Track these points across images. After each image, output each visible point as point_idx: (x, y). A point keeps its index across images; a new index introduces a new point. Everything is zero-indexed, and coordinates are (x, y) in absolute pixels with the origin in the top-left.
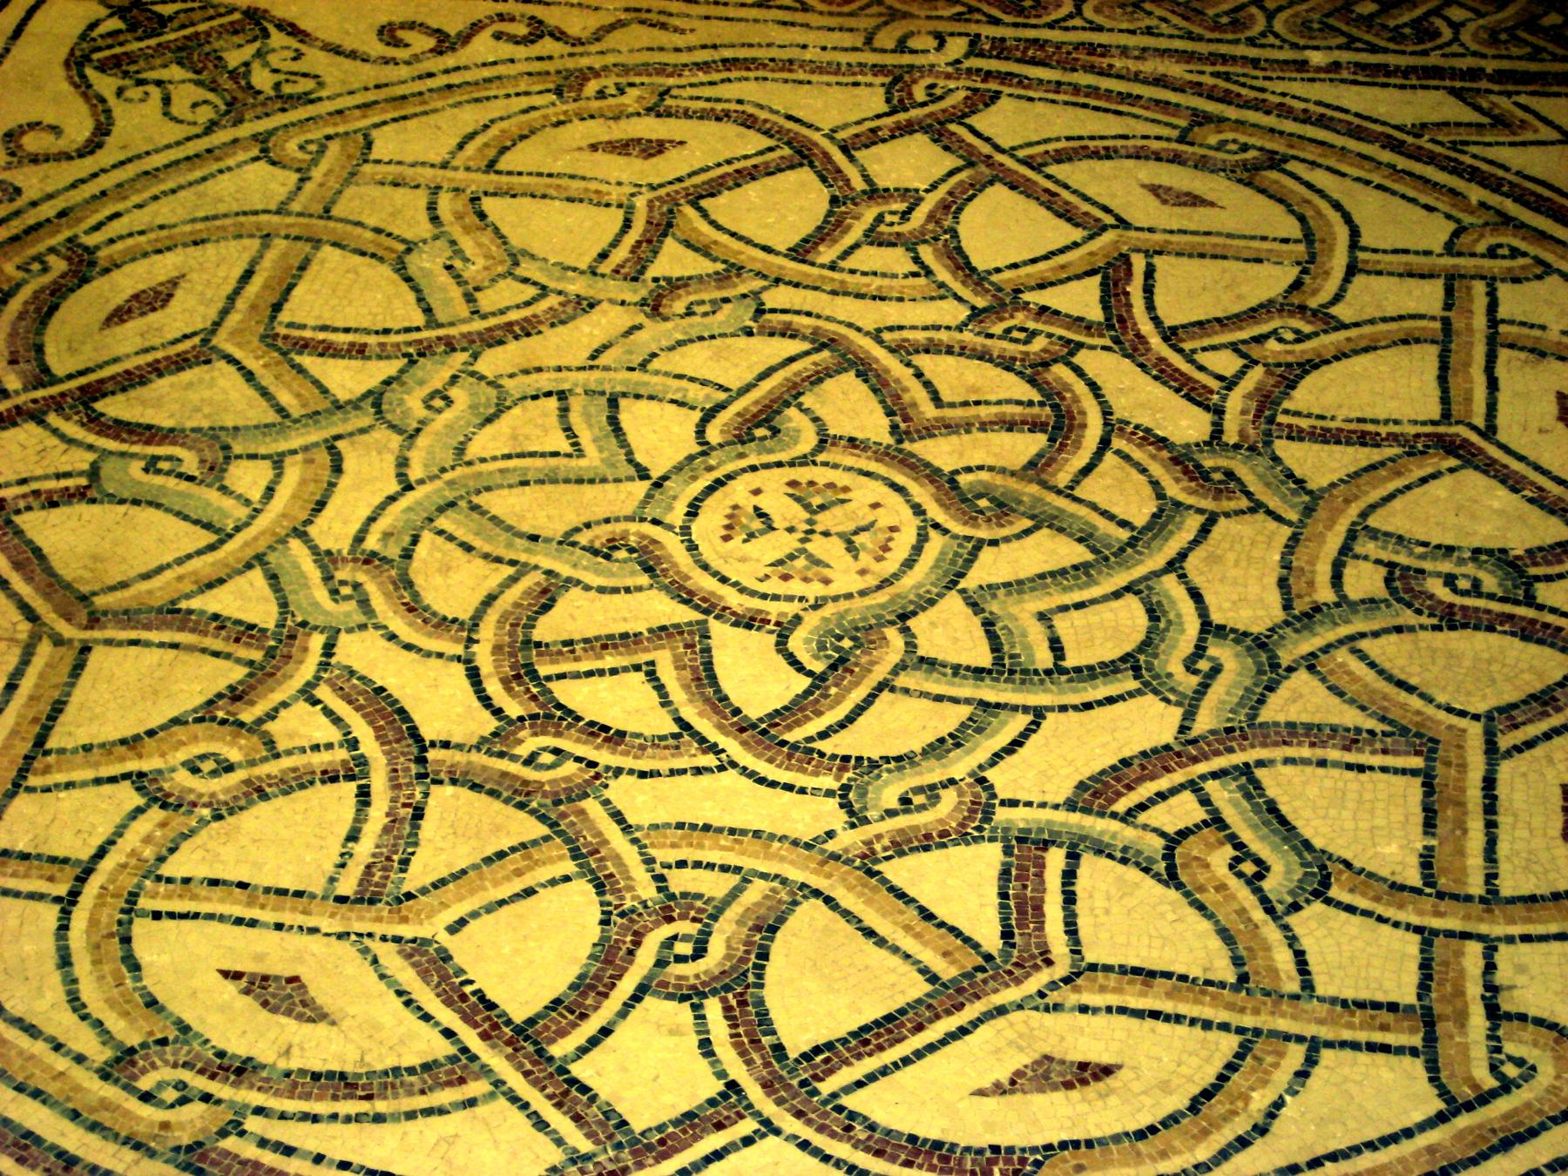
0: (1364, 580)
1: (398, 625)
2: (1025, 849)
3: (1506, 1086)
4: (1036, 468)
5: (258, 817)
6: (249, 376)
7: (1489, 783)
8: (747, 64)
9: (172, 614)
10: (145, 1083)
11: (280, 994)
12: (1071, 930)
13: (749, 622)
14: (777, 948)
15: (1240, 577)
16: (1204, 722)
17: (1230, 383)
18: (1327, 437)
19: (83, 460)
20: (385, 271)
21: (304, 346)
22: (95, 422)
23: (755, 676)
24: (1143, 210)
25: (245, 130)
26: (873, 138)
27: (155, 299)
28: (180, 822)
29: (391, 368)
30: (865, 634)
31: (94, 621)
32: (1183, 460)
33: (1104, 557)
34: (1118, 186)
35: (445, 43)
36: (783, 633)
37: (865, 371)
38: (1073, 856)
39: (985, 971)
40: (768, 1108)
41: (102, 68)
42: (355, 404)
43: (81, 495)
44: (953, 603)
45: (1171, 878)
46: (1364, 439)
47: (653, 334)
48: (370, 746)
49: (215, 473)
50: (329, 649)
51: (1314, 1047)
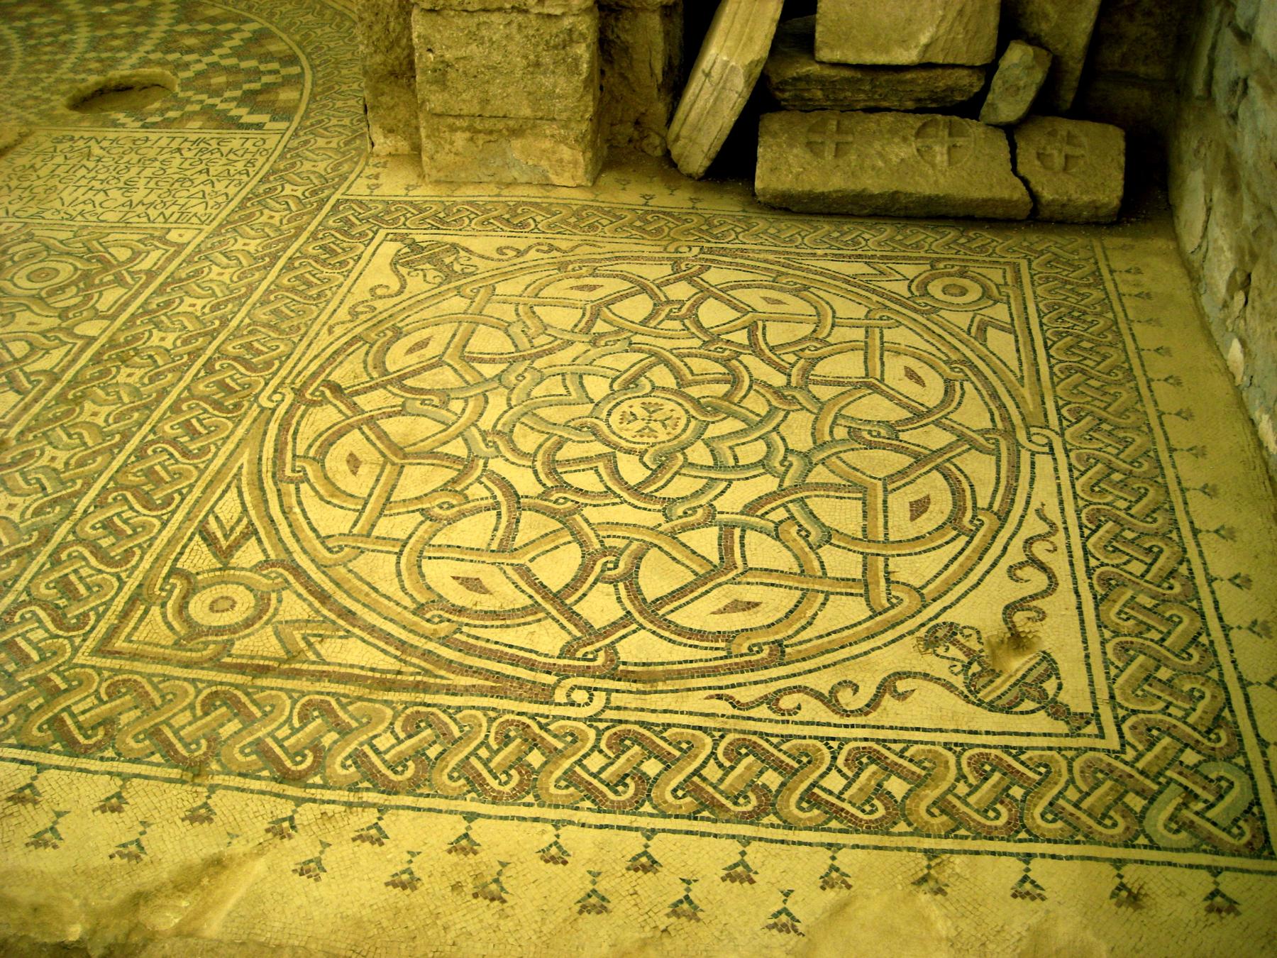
0: (841, 433)
1: (509, 455)
3: (893, 606)
4: (727, 396)
5: (463, 524)
7: (885, 502)
8: (624, 258)
9: (432, 454)
10: (428, 616)
11: (472, 584)
12: (744, 556)
15: (798, 432)
16: (787, 484)
17: (793, 365)
19: (399, 401)
20: (501, 333)
21: (474, 359)
22: (403, 387)
23: (633, 471)
24: (761, 306)
25: (452, 285)
26: (668, 283)
27: (423, 344)
28: (437, 525)
30: (670, 456)
31: (405, 456)
33: (752, 427)
34: (752, 297)
35: (520, 253)
36: (642, 455)
37: (667, 363)
38: (743, 531)
39: (714, 572)
40: (641, 620)
43: (399, 413)
44: (700, 443)
45: (777, 538)
46: (839, 384)
47: (594, 352)
48: (500, 498)
49: (445, 404)
50: (485, 465)
51: (827, 594)
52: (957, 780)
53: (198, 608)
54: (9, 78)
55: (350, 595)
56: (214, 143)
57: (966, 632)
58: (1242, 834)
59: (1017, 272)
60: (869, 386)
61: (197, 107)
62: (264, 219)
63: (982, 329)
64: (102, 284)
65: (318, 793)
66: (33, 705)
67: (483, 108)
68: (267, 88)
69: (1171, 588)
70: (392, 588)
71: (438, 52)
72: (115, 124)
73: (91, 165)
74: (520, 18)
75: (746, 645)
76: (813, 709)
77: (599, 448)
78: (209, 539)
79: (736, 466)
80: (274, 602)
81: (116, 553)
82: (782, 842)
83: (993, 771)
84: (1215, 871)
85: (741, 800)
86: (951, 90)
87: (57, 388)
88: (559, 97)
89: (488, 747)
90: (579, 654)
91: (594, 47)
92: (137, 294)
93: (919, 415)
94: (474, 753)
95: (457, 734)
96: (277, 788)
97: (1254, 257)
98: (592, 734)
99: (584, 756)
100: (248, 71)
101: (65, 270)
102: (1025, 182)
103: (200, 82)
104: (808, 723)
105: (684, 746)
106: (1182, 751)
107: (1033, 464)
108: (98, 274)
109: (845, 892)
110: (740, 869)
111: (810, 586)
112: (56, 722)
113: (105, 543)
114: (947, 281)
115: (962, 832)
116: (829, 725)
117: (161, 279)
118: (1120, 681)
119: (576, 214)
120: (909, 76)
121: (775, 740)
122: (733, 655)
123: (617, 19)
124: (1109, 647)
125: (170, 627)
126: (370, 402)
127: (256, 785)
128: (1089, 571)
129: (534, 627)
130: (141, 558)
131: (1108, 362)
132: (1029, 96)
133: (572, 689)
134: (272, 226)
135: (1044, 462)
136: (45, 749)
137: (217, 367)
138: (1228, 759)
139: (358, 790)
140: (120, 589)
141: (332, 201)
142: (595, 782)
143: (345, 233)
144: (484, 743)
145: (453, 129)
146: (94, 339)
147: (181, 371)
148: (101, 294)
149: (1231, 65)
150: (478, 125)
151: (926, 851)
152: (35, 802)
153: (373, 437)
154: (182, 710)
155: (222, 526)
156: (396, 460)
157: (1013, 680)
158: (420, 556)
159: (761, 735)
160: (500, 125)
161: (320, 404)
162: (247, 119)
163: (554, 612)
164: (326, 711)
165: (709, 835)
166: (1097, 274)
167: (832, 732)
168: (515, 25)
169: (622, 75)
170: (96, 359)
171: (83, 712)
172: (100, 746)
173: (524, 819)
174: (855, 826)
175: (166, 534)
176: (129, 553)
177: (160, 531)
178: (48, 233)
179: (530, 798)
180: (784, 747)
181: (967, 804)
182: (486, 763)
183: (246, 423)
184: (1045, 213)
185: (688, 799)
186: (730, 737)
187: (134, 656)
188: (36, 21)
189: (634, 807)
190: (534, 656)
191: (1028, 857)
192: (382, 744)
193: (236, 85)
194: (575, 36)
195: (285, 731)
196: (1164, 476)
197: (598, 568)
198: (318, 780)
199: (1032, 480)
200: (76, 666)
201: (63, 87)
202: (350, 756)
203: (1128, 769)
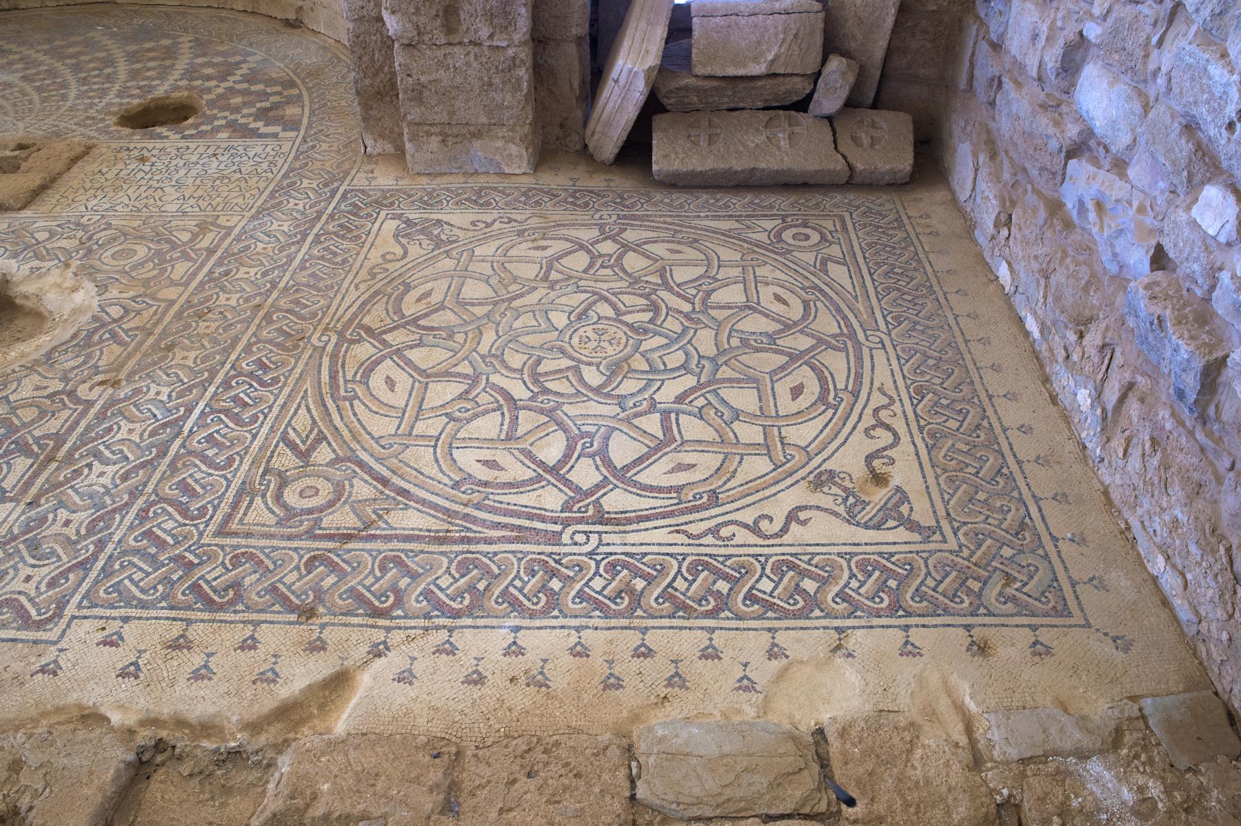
0: (735, 342)
1: (503, 371)
2: (666, 414)
3: (788, 461)
4: (652, 321)
7: (773, 389)
8: (564, 225)
9: (447, 374)
11: (491, 464)
12: (680, 432)
13: (589, 364)
14: (610, 443)
15: (705, 341)
16: (702, 380)
17: (695, 296)
18: (721, 308)
19: (417, 336)
21: (467, 304)
22: (418, 327)
23: (593, 377)
24: (666, 255)
26: (598, 242)
27: (428, 294)
28: (459, 425)
29: (490, 307)
31: (428, 376)
32: (687, 316)
33: (673, 341)
34: (659, 250)
35: (488, 225)
37: (606, 300)
42: (483, 317)
44: (638, 355)
45: (701, 418)
46: (729, 308)
47: (553, 294)
48: (502, 402)
49: (451, 336)
50: (487, 379)
51: (742, 456)
52: (850, 578)
53: (290, 497)
54: (69, 104)
57: (842, 475)
58: (1049, 601)
59: (843, 221)
60: (750, 308)
61: (224, 122)
62: (291, 205)
63: (824, 263)
65: (402, 622)
66: (175, 577)
67: (450, 118)
68: (275, 106)
69: (978, 437)
70: (433, 471)
73: (147, 169)
75: (691, 494)
76: (743, 536)
77: (568, 363)
78: (292, 446)
79: (666, 370)
80: (347, 487)
82: (737, 629)
83: (874, 570)
84: (1034, 628)
85: (704, 602)
86: (789, 92)
87: (151, 340)
89: (521, 579)
90: (575, 509)
91: (531, 70)
93: (787, 327)
94: (511, 583)
95: (497, 571)
96: (371, 621)
97: (1013, 203)
98: (593, 564)
99: (590, 580)
101: (142, 252)
102: (845, 157)
103: (222, 102)
104: (742, 546)
105: (659, 567)
106: (1001, 548)
107: (872, 356)
108: (168, 252)
109: (784, 661)
110: (710, 650)
111: (729, 450)
112: (195, 587)
113: (210, 453)
114: (795, 230)
115: (859, 613)
116: (756, 546)
117: (219, 254)
118: (952, 503)
119: (525, 194)
120: (760, 84)
121: (721, 559)
122: (681, 504)
123: (544, 49)
124: (942, 482)
125: (273, 512)
126: (396, 338)
127: (355, 620)
128: (921, 429)
130: (241, 463)
131: (914, 282)
132: (844, 94)
133: (574, 533)
134: (298, 211)
135: (879, 356)
136: (189, 608)
138: (1033, 551)
139: (431, 618)
140: (228, 486)
142: (600, 597)
143: (355, 214)
144: (517, 576)
145: (429, 134)
146: (172, 302)
147: (248, 321)
148: (173, 266)
149: (986, 66)
150: (447, 130)
151: (836, 629)
152: (189, 648)
153: (402, 364)
154: (291, 571)
155: (299, 435)
157: (878, 507)
158: (450, 447)
159: (710, 556)
160: (464, 131)
161: (358, 341)
162: (263, 130)
163: (553, 480)
164: (399, 562)
165: (685, 628)
166: (898, 219)
167: (758, 550)
168: (472, 55)
169: (549, 90)
170: (179, 316)
171: (215, 579)
172: (232, 603)
173: (554, 628)
174: (786, 614)
176: (230, 460)
177: (252, 442)
178: (124, 223)
179: (556, 613)
180: (727, 563)
181: (860, 594)
182: (521, 590)
183: (306, 355)
184: (858, 179)
185: (667, 604)
186: (689, 559)
187: (249, 535)
188: (83, 58)
189: (630, 612)
190: (543, 512)
191: (906, 628)
193: (251, 104)
194: (517, 62)
195: (370, 580)
196: (964, 359)
197: (579, 447)
198: (400, 612)
199: (873, 367)
200: (203, 545)
202: (421, 594)
203: (966, 563)
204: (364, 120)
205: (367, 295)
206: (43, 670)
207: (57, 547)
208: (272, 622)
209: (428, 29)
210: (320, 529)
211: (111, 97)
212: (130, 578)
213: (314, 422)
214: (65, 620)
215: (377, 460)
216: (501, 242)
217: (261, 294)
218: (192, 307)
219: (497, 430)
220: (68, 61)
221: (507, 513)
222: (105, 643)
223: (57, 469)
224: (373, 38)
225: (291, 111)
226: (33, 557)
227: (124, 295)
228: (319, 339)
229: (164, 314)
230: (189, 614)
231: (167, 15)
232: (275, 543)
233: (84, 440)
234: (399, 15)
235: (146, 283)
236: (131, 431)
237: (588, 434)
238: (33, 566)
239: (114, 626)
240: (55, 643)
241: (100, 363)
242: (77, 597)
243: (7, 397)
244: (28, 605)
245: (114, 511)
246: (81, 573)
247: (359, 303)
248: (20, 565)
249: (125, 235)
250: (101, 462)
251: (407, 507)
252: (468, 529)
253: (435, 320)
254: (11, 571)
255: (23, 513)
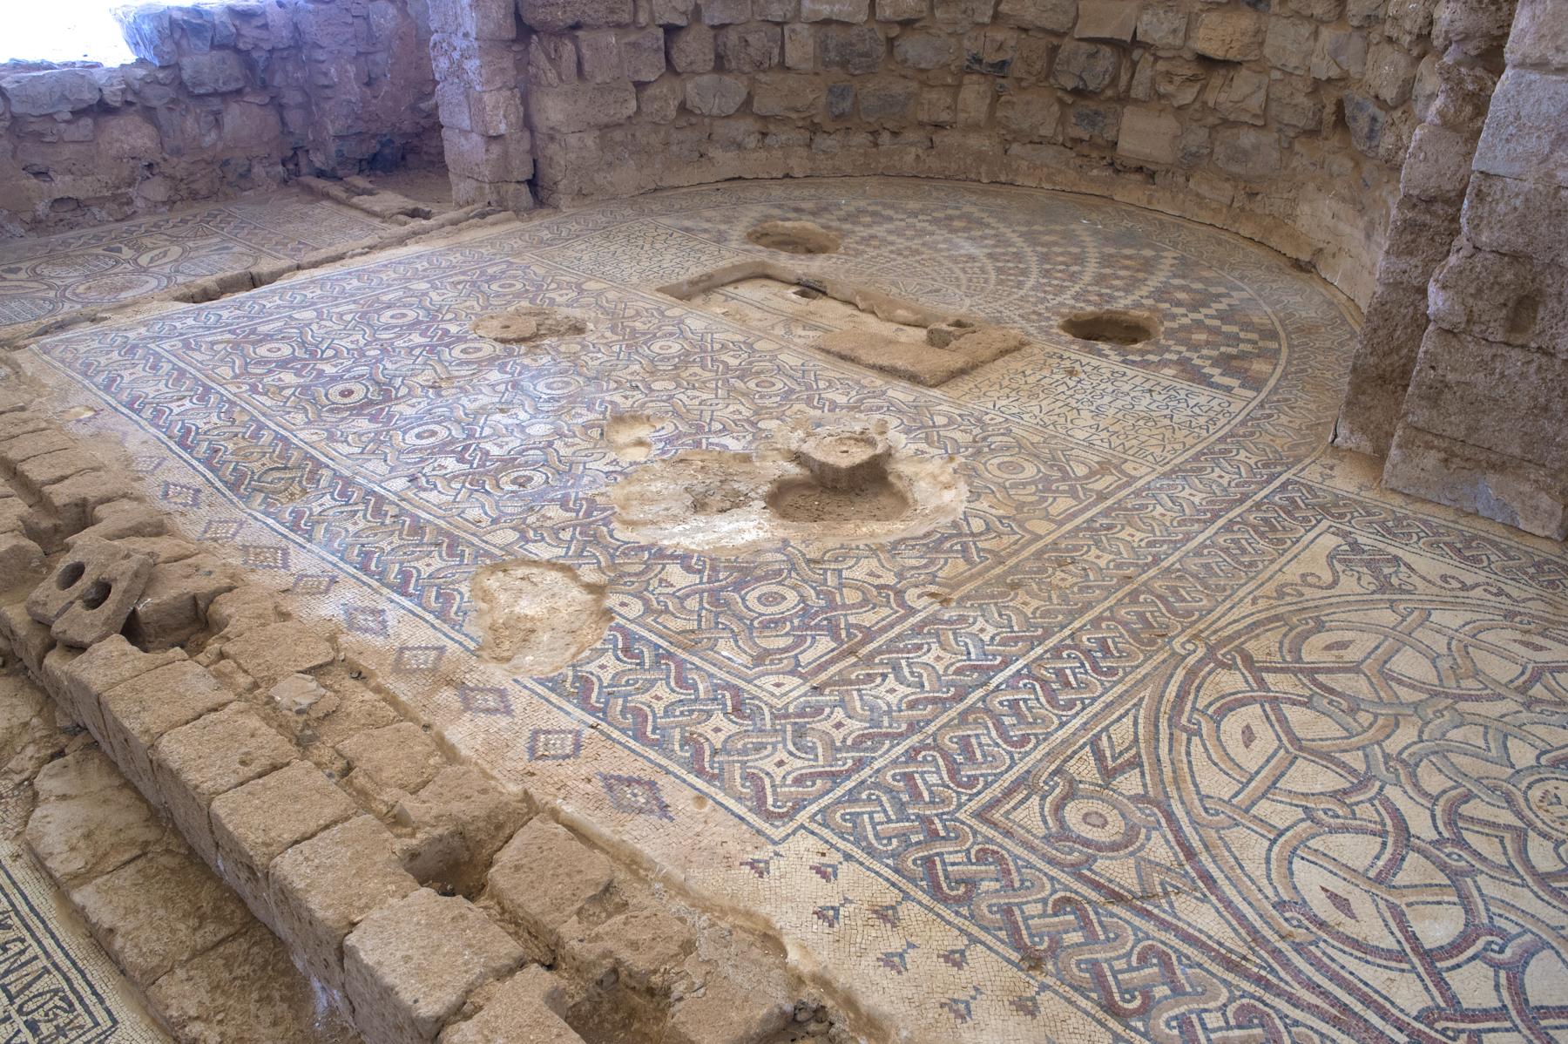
6: (1371, 683)
10: (1287, 915)
13: (1545, 836)
14: (1533, 962)
19: (1307, 693)
20: (1427, 662)
21: (1393, 679)
22: (1314, 681)
25: (1386, 597)
28: (1316, 829)
31: (1301, 749)
35: (1464, 587)
40: (1518, 1021)
41: (1339, 561)
42: (1408, 705)
43: (1304, 704)
48: (1390, 828)
49: (1353, 711)
50: (1381, 788)
54: (1022, 293)
55: (1214, 861)
56: (1183, 393)
61: (1175, 357)
62: (1214, 475)
64: (1057, 491)
66: (914, 839)
67: (1468, 436)
68: (1243, 356)
70: (1259, 872)
71: (1440, 372)
72: (1100, 354)
73: (1071, 384)
74: (1544, 360)
78: (1099, 756)
80: (1142, 836)
81: (1015, 734)
87: (999, 570)
88: (1558, 445)
90: (1439, 1025)
92: (1086, 509)
96: (1101, 1015)
100: (1228, 336)
101: (1030, 471)
103: (1182, 335)
108: (1057, 481)
112: (928, 862)
113: (1007, 721)
117: (1109, 502)
119: (1538, 565)
125: (1045, 822)
126: (1279, 683)
127: (1083, 1003)
129: (1395, 975)
130: (1035, 748)
134: (1220, 485)
136: (912, 880)
137: (1141, 598)
140: (1010, 768)
141: (1284, 478)
143: (1288, 513)
145: (1429, 446)
146: (1040, 537)
147: (1110, 591)
150: (1457, 449)
152: (894, 926)
153: (1273, 718)
154: (1036, 901)
155: (1112, 747)
156: (1291, 749)
161: (1230, 667)
162: (1217, 379)
163: (1421, 970)
164: (1165, 963)
168: (1534, 366)
170: (1039, 555)
171: (953, 864)
172: (958, 900)
175: (1061, 734)
176: (1024, 739)
177: (1056, 730)
183: (1160, 657)
187: (1008, 834)
188: (1056, 249)
190: (1388, 1005)
192: (1213, 1020)
193: (1215, 346)
197: (1480, 944)
198: (1139, 1025)
200: (957, 820)
201: (1065, 310)
202: (1176, 1018)
204: (1348, 403)
205: (1263, 615)
206: (752, 864)
207: (819, 745)
208: (990, 948)
209: (1485, 318)
210: (1090, 870)
211: (1067, 298)
212: (871, 814)
213: (1136, 740)
214: (793, 825)
215: (1192, 822)
216: (1475, 616)
217: (1137, 565)
218: (1056, 550)
219: (1367, 862)
220: (1039, 249)
221: (1334, 977)
222: (818, 871)
223: (854, 665)
224: (1403, 311)
225: (1259, 366)
226: (795, 744)
227: (993, 511)
228: (1183, 645)
229: (1024, 547)
230: (909, 887)
231: (1161, 223)
232: (1033, 859)
233: (890, 647)
234: (1451, 293)
235: (1020, 506)
236: (938, 658)
237: (1502, 933)
238: (791, 753)
239: (834, 857)
240: (775, 843)
241: (940, 574)
242: (814, 808)
243: (840, 571)
244: (769, 791)
245: (887, 735)
246: (829, 784)
247: (1249, 620)
248: (780, 746)
249: (1020, 447)
250: (897, 679)
251: (1204, 900)
252: (1273, 971)
253: (1340, 682)
254: (770, 747)
255: (805, 695)
